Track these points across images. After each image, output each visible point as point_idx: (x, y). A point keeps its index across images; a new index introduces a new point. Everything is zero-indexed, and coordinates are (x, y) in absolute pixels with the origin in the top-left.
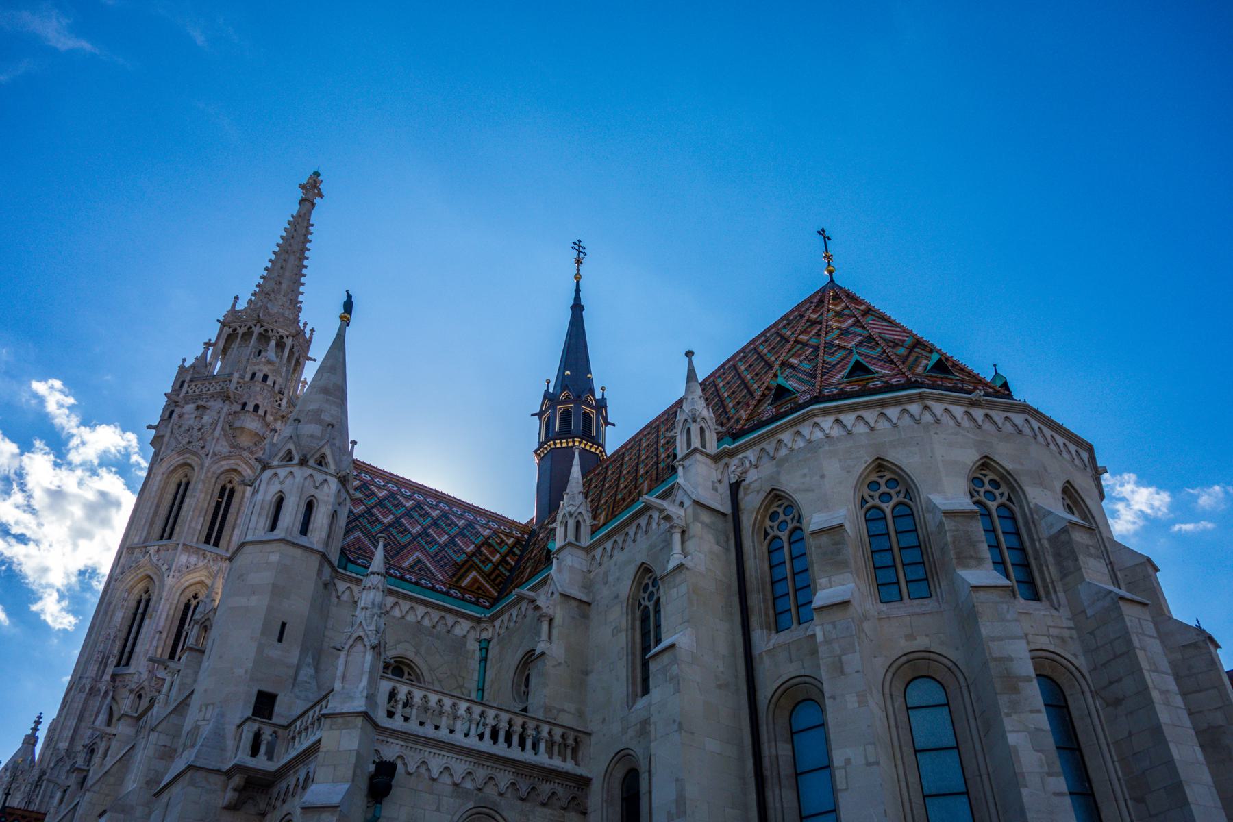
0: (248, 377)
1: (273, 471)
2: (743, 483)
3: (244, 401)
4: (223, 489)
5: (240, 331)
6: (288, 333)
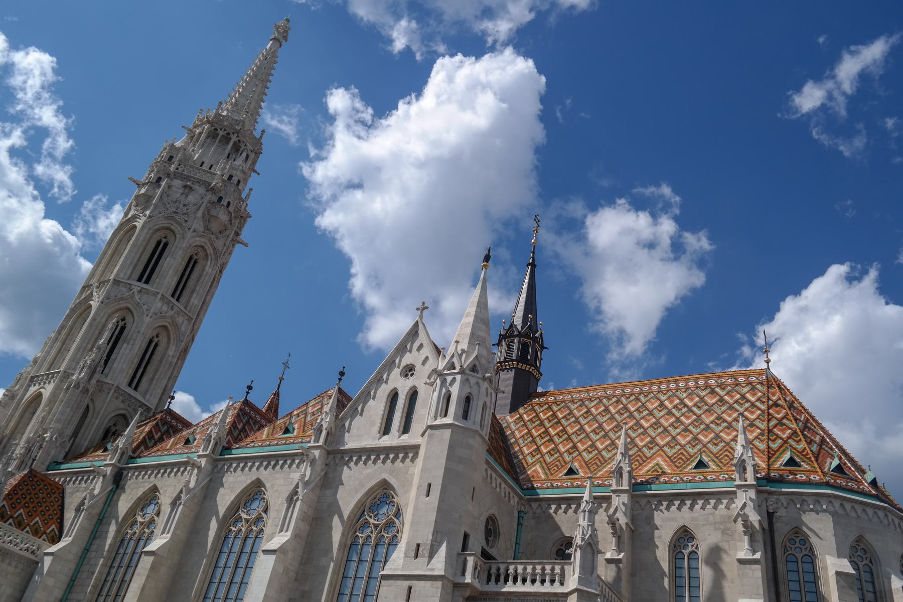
0: (225, 178)
1: (466, 377)
2: (775, 514)
3: (221, 195)
5: (221, 133)
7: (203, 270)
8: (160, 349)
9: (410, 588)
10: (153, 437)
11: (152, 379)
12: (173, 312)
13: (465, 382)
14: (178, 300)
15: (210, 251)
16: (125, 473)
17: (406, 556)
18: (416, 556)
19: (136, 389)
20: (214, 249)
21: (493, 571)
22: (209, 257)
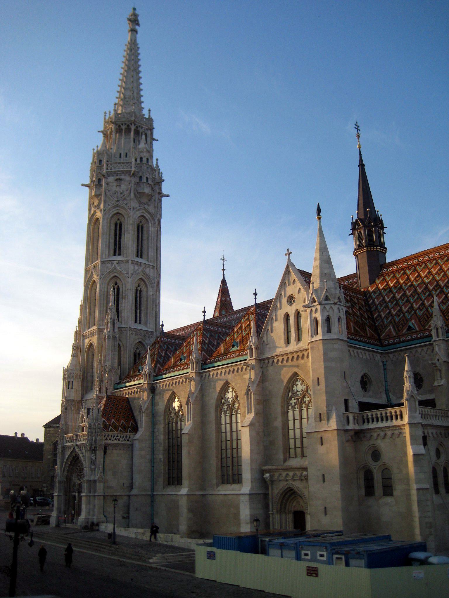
0: (138, 161)
1: (323, 306)
3: (140, 175)
5: (124, 127)
6: (147, 128)
7: (148, 231)
8: (144, 293)
9: (322, 438)
10: (161, 355)
11: (147, 314)
12: (141, 268)
13: (323, 309)
14: (141, 257)
16: (155, 386)
17: (316, 421)
18: (321, 420)
19: (140, 323)
20: (150, 213)
21: (365, 417)
22: (150, 221)
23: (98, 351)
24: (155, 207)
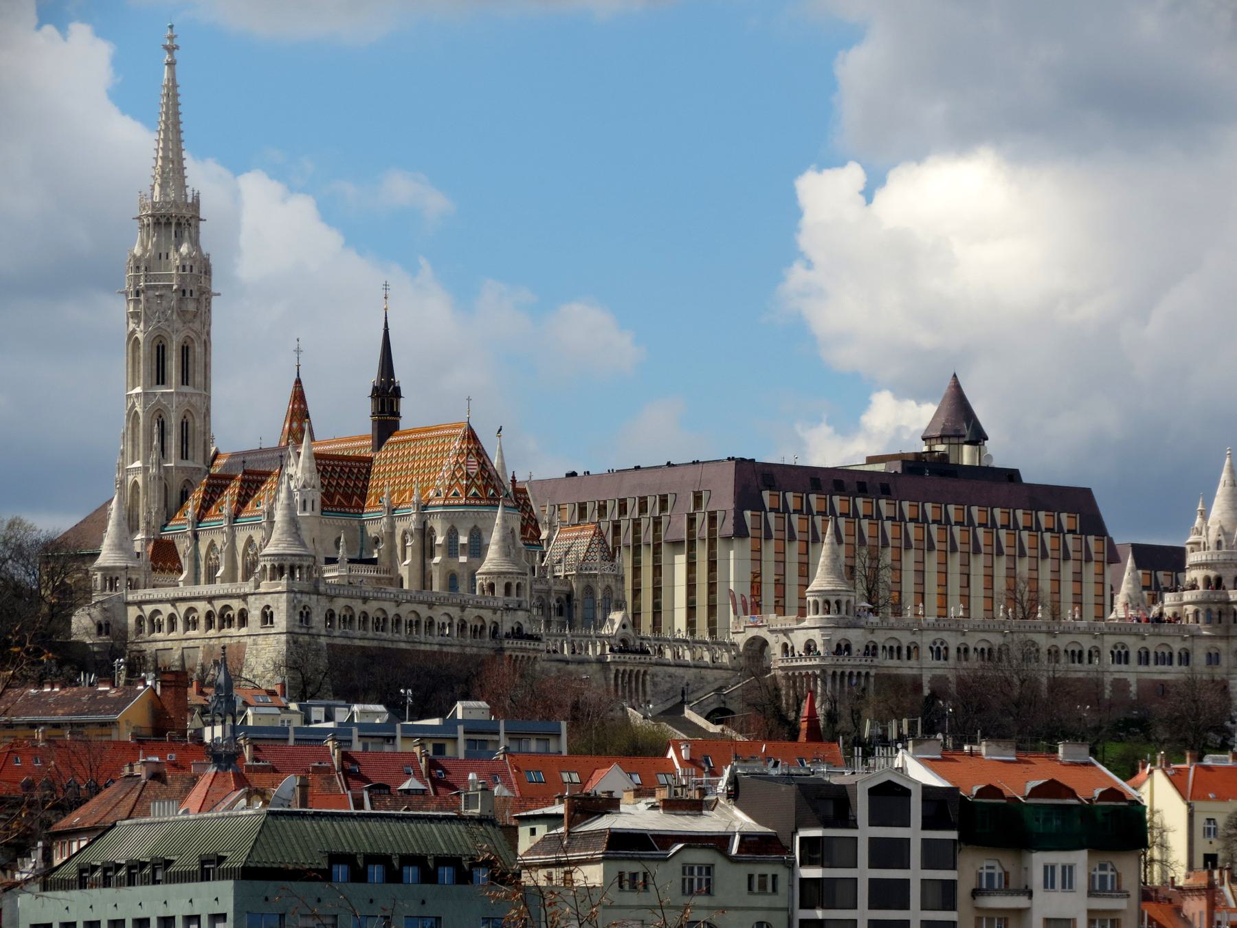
4: (183, 347)
5: (163, 221)
7: (194, 352)
8: (190, 425)
11: (194, 448)
12: (187, 399)
15: (193, 335)
20: (195, 332)
23: (144, 491)
24: (201, 322)
